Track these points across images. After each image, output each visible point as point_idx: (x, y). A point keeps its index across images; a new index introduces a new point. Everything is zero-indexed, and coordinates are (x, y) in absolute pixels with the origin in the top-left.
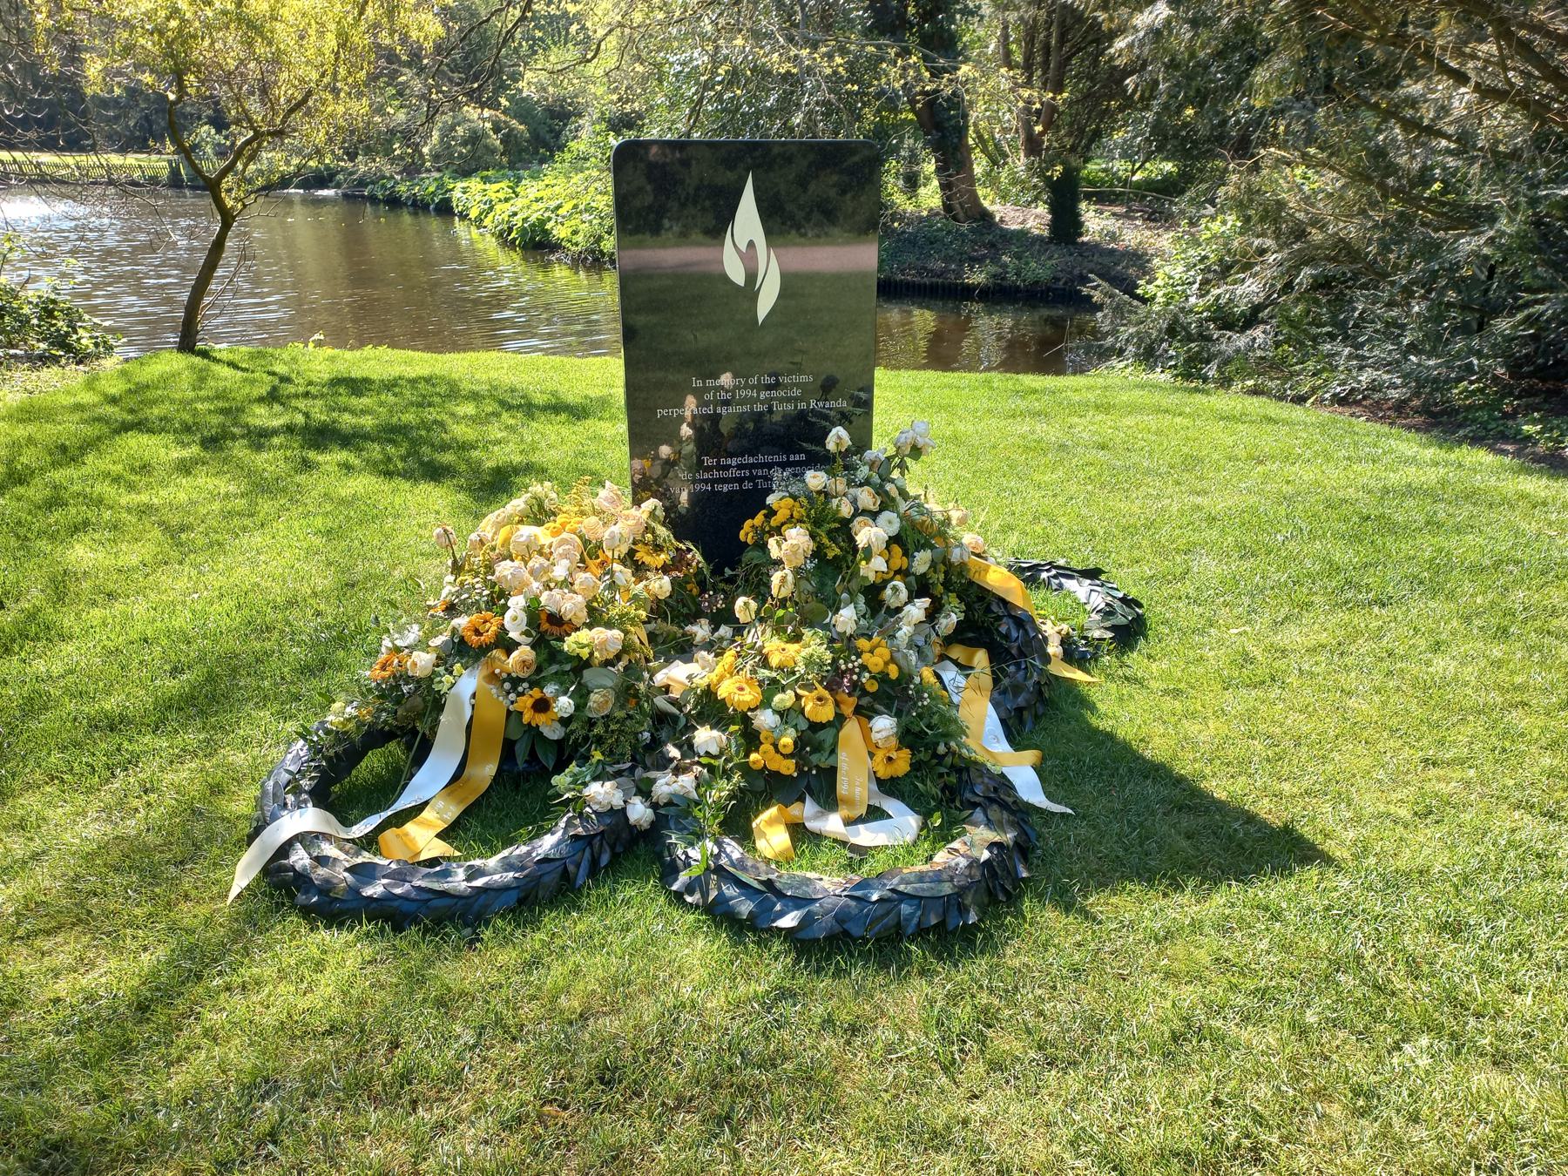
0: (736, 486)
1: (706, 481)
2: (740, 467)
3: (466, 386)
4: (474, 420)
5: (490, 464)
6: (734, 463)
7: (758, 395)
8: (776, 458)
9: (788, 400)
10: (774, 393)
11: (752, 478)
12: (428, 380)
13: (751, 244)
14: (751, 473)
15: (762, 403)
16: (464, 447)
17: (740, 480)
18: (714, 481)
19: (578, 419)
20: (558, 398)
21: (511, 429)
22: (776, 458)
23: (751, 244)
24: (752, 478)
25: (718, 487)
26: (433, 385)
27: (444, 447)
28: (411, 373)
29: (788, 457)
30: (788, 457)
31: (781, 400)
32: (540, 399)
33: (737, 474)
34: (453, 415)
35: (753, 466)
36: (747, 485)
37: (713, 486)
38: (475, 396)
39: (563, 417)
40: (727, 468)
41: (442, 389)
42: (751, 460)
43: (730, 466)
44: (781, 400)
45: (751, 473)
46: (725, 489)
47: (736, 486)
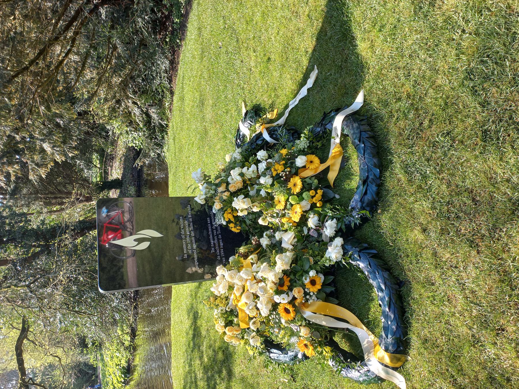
0: (221, 241)
1: (220, 251)
2: (214, 240)
6: (213, 242)
10: (187, 230)
11: (217, 235)
13: (135, 240)
14: (215, 236)
15: (190, 233)
17: (218, 239)
23: (135, 240)
24: (217, 235)
25: (222, 247)
29: (209, 224)
30: (209, 224)
33: (216, 240)
36: (220, 236)
37: (222, 249)
40: (214, 244)
43: (214, 243)
45: (215, 236)
46: (222, 244)
47: (221, 241)
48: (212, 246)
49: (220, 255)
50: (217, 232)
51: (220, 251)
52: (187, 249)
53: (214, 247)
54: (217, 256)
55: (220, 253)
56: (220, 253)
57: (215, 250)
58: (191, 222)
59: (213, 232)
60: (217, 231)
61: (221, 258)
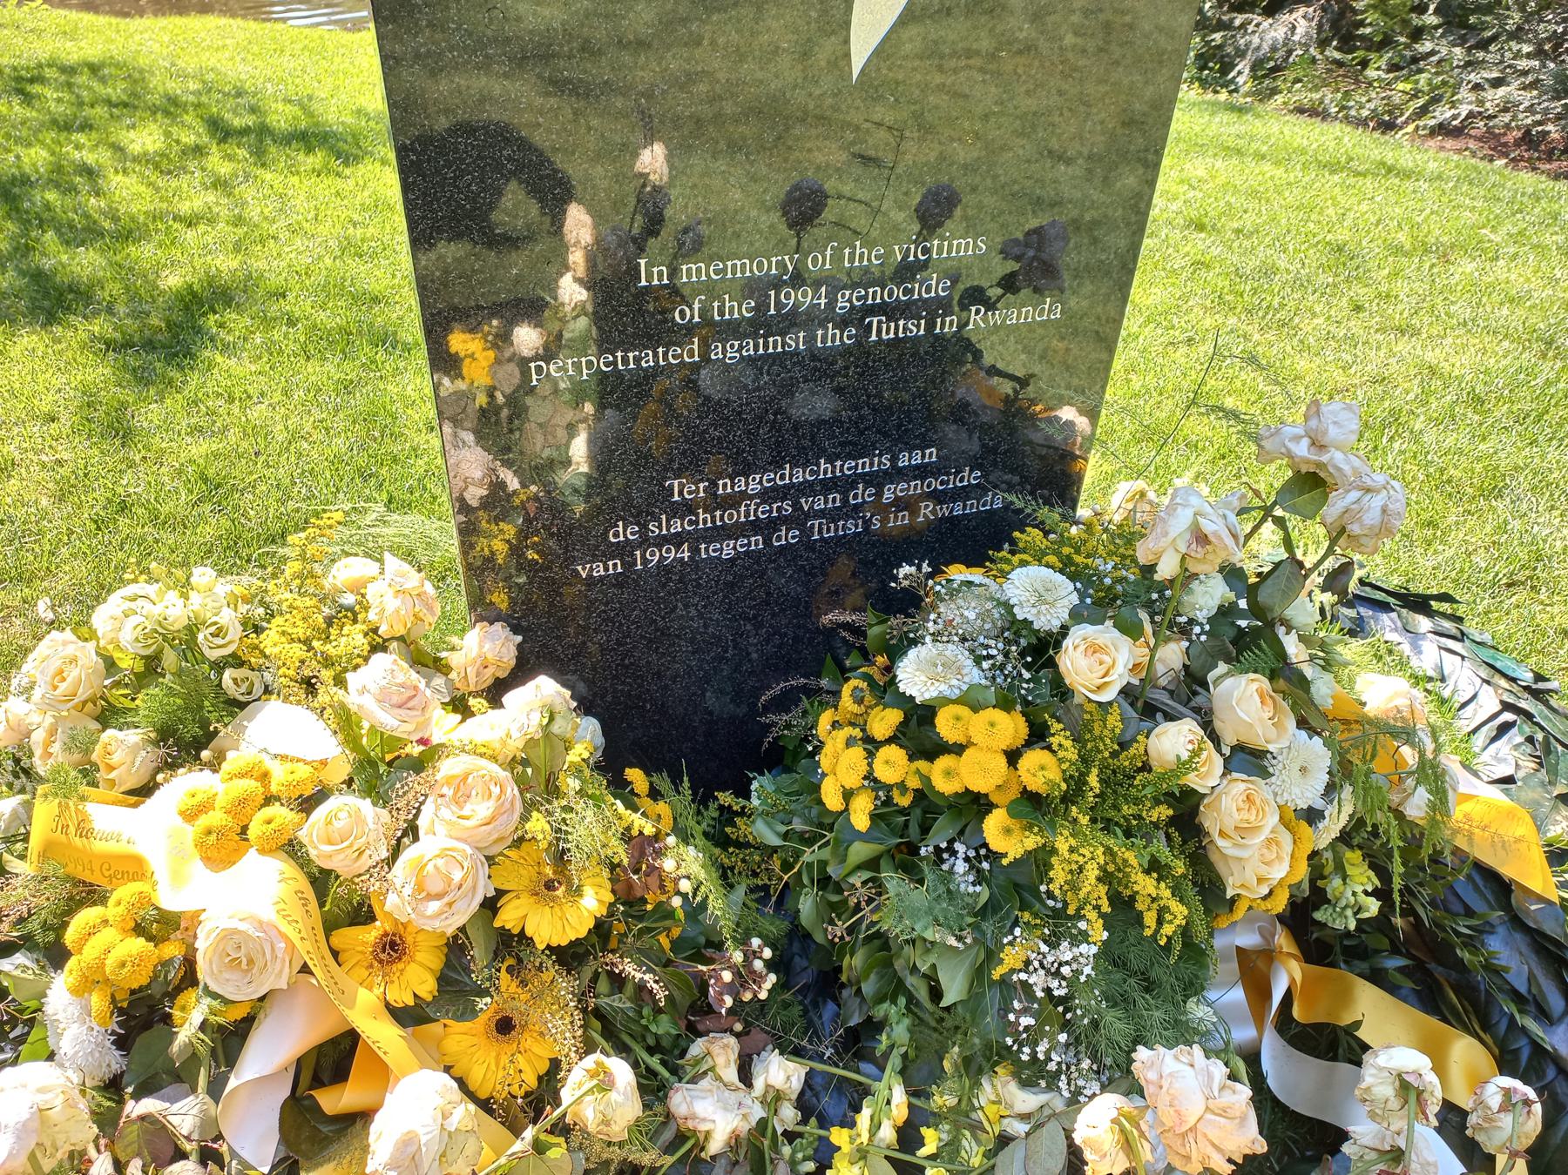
0: (757, 542)
1: (677, 540)
2: (767, 496)
3: (161, 85)
4: (160, 164)
5: (172, 281)
6: (754, 487)
7: (832, 303)
8: (864, 465)
11: (799, 519)
12: (94, 69)
14: (797, 506)
15: (843, 324)
16: (128, 233)
17: (766, 528)
18: (694, 539)
19: (346, 163)
20: (310, 115)
21: (221, 184)
22: (864, 465)
24: (799, 519)
25: (707, 551)
26: (103, 80)
27: (83, 233)
28: (73, 52)
29: (894, 459)
30: (894, 459)
31: (891, 311)
32: (281, 116)
34: (118, 149)
35: (807, 489)
36: (787, 537)
37: (695, 550)
38: (171, 108)
39: (317, 159)
40: (733, 501)
41: (116, 91)
42: (800, 476)
43: (744, 495)
44: (891, 311)
45: (797, 506)
46: (728, 550)
47: (757, 542)
48: (724, 487)
49: (645, 541)
50: (822, 514)
51: (677, 540)
53: (716, 502)
54: (640, 516)
55: (661, 541)
56: (661, 541)
57: (688, 508)
58: (931, 326)
59: (827, 486)
60: (832, 516)
61: (623, 551)
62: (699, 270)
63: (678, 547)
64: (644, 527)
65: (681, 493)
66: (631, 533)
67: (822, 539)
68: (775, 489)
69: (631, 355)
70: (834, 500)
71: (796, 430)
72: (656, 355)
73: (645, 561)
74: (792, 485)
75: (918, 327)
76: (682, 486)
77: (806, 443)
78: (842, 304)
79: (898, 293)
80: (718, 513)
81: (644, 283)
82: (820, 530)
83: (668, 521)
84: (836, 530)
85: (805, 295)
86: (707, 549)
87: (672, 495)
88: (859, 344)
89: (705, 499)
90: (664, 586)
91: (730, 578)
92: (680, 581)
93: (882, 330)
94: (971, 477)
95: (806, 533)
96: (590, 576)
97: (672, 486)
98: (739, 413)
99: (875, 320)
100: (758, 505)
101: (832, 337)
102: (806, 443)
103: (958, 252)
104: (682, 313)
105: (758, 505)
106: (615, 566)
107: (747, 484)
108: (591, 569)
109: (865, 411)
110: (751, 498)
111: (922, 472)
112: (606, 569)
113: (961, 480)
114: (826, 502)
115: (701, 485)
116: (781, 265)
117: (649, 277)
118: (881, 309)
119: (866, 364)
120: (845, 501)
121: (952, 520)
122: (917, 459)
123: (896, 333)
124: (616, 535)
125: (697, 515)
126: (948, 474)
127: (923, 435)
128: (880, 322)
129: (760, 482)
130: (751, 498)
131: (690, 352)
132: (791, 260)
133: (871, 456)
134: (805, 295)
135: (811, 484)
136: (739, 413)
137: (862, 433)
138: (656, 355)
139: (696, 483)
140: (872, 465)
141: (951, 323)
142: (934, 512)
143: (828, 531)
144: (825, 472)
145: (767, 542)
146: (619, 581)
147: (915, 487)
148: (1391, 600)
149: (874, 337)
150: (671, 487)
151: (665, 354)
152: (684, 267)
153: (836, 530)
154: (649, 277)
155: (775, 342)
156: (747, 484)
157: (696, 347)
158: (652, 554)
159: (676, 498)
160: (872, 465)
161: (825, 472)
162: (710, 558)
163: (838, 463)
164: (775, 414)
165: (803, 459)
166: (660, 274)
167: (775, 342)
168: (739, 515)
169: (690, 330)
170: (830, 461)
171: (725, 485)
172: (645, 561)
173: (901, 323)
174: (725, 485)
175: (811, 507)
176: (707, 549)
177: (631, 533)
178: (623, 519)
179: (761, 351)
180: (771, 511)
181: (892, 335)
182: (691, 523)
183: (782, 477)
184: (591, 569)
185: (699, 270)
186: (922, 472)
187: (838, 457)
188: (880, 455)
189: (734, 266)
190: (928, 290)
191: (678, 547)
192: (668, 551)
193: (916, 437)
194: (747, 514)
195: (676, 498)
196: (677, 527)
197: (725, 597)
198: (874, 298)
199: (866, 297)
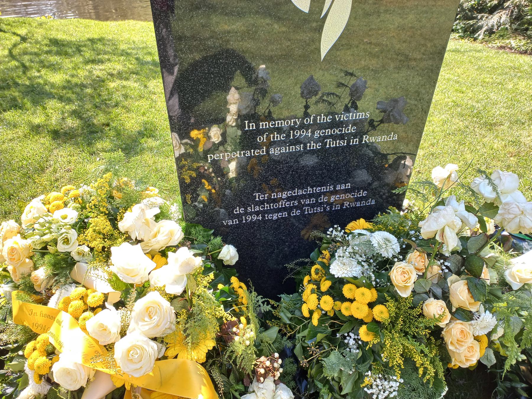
0: (285, 214)
1: (257, 213)
2: (289, 199)
6: (284, 196)
9: (342, 137)
10: (329, 132)
11: (300, 207)
14: (299, 202)
15: (316, 142)
17: (289, 210)
18: (263, 213)
22: (324, 189)
24: (300, 207)
25: (269, 217)
29: (335, 187)
30: (335, 187)
31: (334, 137)
35: (303, 197)
36: (296, 213)
37: (263, 217)
42: (300, 193)
44: (334, 137)
45: (299, 202)
46: (275, 217)
47: (285, 214)
48: (274, 196)
49: (246, 213)
51: (257, 213)
52: (270, 131)
54: (245, 206)
55: (251, 214)
56: (251, 214)
57: (262, 202)
59: (310, 196)
60: (312, 206)
61: (239, 216)
62: (266, 125)
63: (258, 215)
64: (246, 209)
65: (259, 198)
66: (242, 210)
67: (308, 214)
68: (292, 196)
69: (242, 152)
70: (313, 201)
71: (299, 177)
72: (251, 152)
73: (246, 220)
74: (298, 196)
75: (344, 143)
76: (259, 195)
77: (304, 181)
78: (316, 135)
79: (337, 131)
80: (272, 205)
81: (247, 129)
82: (308, 211)
83: (254, 207)
84: (314, 211)
85: (303, 132)
86: (268, 216)
87: (256, 198)
88: (322, 148)
89: (267, 200)
90: (253, 228)
91: (276, 226)
92: (258, 226)
93: (330, 144)
94: (364, 194)
95: (303, 211)
96: (227, 224)
97: (256, 195)
98: (279, 172)
99: (328, 140)
100: (286, 202)
101: (314, 146)
102: (304, 181)
103: (359, 117)
104: (260, 139)
105: (286, 202)
106: (236, 221)
107: (282, 195)
108: (228, 222)
109: (325, 171)
110: (283, 199)
111: (346, 191)
112: (233, 222)
113: (360, 194)
114: (310, 201)
115: (266, 195)
116: (295, 123)
117: (249, 127)
118: (331, 136)
119: (325, 155)
120: (317, 201)
121: (356, 207)
122: (343, 187)
123: (336, 145)
124: (236, 211)
125: (264, 205)
126: (355, 192)
127: (346, 179)
128: (330, 141)
129: (287, 195)
130: (283, 199)
131: (262, 152)
132: (298, 121)
133: (326, 186)
134: (303, 132)
135: (305, 195)
136: (279, 172)
137: (323, 178)
138: (251, 152)
139: (264, 195)
140: (327, 189)
141: (356, 141)
142: (349, 205)
143: (311, 211)
144: (310, 191)
145: (289, 214)
146: (236, 227)
147: (343, 196)
148: (527, 238)
149: (328, 146)
150: (256, 196)
151: (254, 152)
152: (261, 124)
153: (314, 211)
154: (249, 127)
155: (293, 148)
156: (282, 195)
157: (265, 150)
158: (249, 218)
159: (257, 199)
160: (327, 189)
161: (310, 191)
162: (269, 219)
163: (315, 188)
164: (292, 172)
165: (302, 187)
166: (253, 126)
167: (293, 148)
168: (280, 205)
169: (263, 144)
170: (312, 187)
171: (274, 196)
172: (246, 220)
173: (338, 141)
174: (274, 196)
175: (305, 203)
176: (268, 216)
177: (242, 210)
178: (239, 206)
179: (287, 151)
180: (290, 204)
181: (334, 146)
182: (262, 208)
183: (294, 193)
184: (228, 222)
185: (266, 125)
186: (346, 191)
187: (314, 186)
188: (330, 186)
189: (278, 123)
190: (348, 130)
191: (258, 215)
192: (254, 217)
193: (343, 180)
194: (282, 205)
195: (257, 199)
196: (257, 209)
197: (274, 232)
198: (328, 133)
199: (325, 133)
